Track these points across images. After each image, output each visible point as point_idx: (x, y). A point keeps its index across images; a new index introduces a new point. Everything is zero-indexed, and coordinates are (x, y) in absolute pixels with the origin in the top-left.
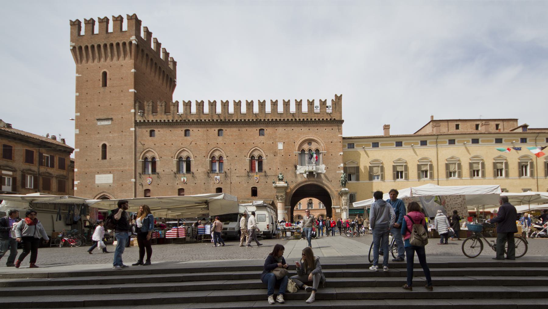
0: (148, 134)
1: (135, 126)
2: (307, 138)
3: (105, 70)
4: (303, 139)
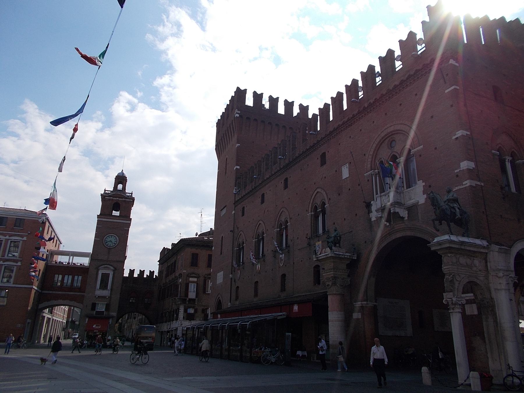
0: (241, 214)
1: (235, 207)
2: (383, 135)
3: (227, 156)
4: (378, 140)
